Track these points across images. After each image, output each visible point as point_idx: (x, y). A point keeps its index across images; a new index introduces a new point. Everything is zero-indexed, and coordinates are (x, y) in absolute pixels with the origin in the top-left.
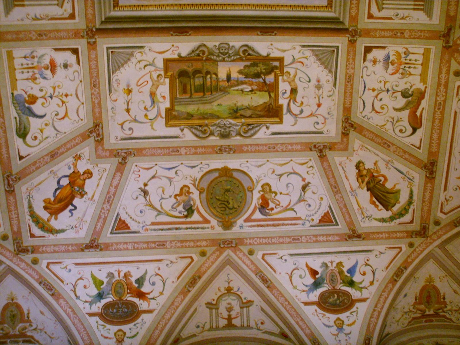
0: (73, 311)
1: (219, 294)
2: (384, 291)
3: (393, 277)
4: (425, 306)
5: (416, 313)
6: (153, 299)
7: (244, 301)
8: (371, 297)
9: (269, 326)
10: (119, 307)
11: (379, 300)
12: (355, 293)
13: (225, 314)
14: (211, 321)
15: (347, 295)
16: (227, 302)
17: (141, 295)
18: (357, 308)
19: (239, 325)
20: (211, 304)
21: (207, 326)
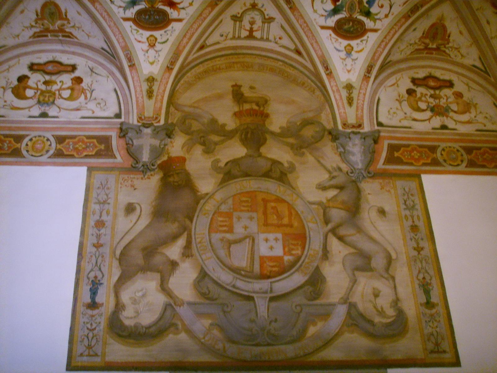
0: (108, 14)
1: (244, 8)
2: (395, 24)
3: (407, 13)
4: (430, 40)
5: (420, 45)
6: (183, 8)
7: (267, 17)
8: (383, 29)
10: (151, 14)
11: (389, 32)
12: (368, 23)
13: (248, 27)
15: (362, 23)
16: (251, 16)
18: (368, 37)
20: (236, 16)
21: (230, 36)
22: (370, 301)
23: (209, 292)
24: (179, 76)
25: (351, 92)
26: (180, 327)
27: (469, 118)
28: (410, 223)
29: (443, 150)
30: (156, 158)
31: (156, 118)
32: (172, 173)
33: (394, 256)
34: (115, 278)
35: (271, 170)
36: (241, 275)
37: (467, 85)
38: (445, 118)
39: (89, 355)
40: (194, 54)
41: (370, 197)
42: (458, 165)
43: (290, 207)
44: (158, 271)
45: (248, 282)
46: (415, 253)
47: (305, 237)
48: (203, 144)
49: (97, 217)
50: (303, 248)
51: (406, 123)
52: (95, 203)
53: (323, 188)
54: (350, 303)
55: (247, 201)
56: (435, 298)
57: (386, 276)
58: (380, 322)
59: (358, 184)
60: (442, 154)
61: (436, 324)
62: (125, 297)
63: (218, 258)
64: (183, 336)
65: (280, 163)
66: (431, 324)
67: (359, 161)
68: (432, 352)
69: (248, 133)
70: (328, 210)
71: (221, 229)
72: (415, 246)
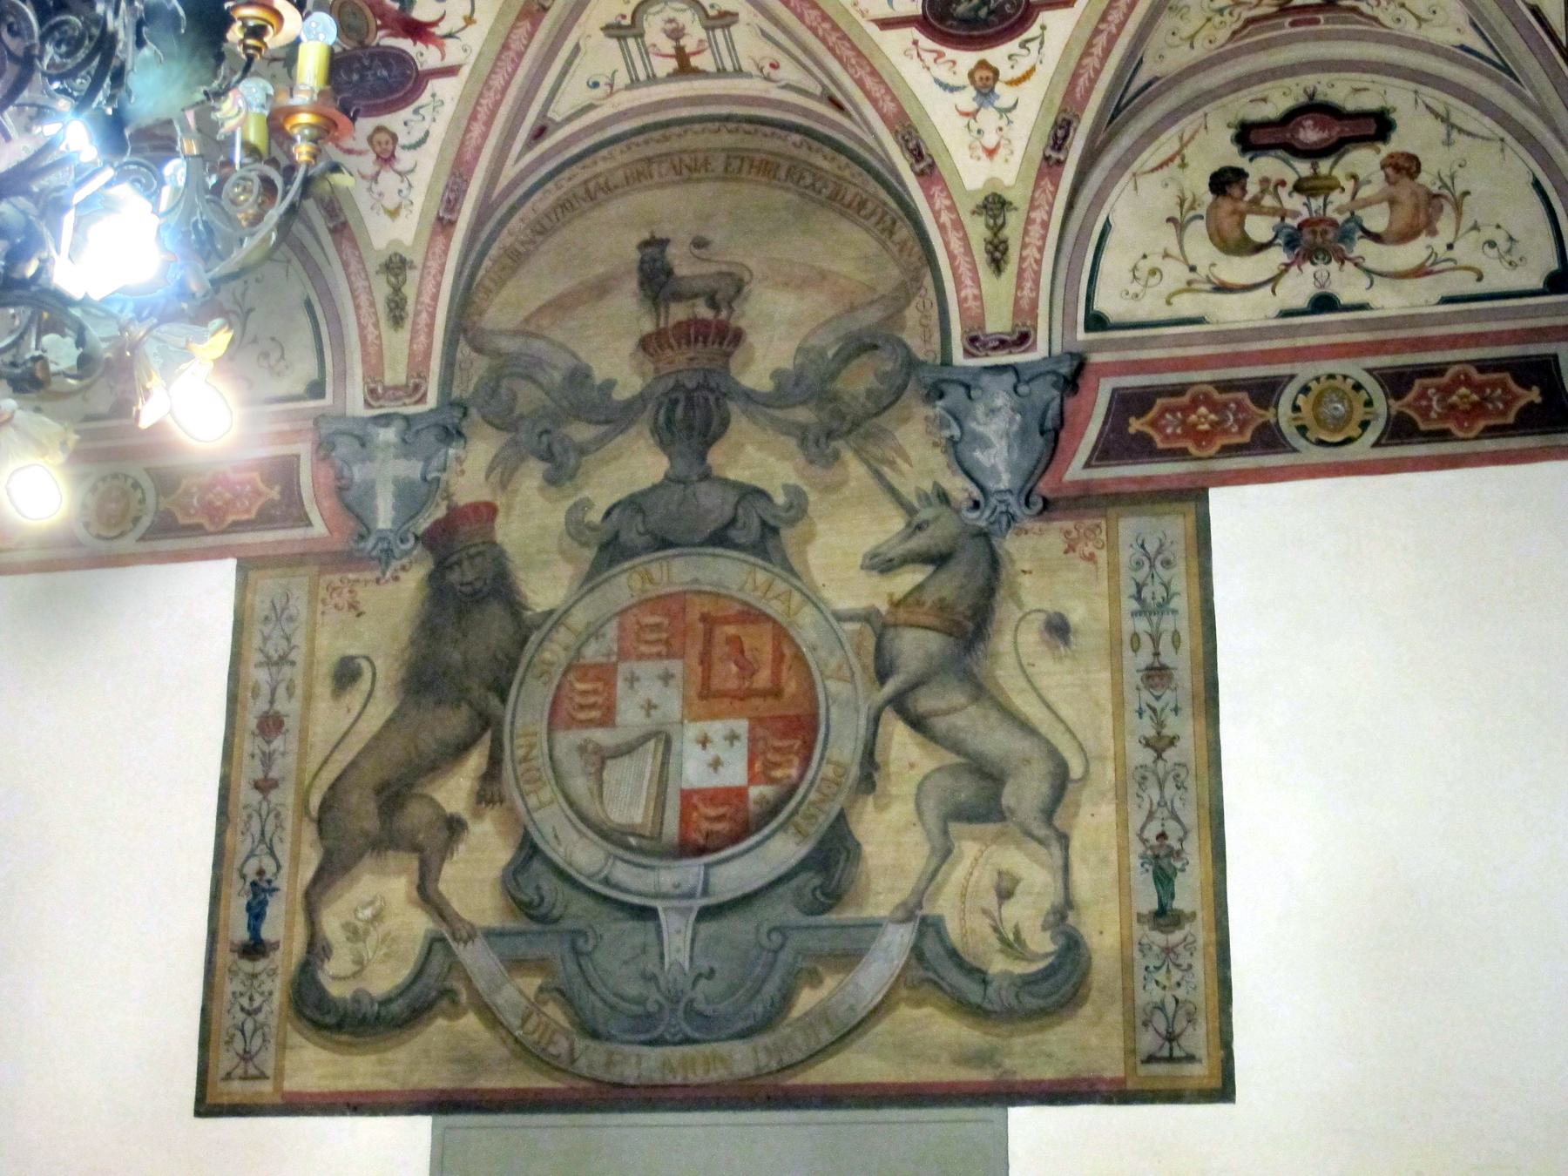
6: (450, 36)
7: (712, 13)
9: (789, 72)
10: (363, 66)
14: (630, 66)
17: (418, 31)
19: (712, 68)
21: (623, 78)
22: (985, 912)
23: (542, 899)
24: (484, 236)
25: (1000, 221)
26: (464, 997)
27: (1425, 254)
28: (1145, 658)
29: (1305, 390)
30: (412, 517)
31: (417, 387)
32: (454, 558)
33: (1076, 769)
34: (308, 873)
35: (733, 522)
36: (629, 848)
37: (1445, 120)
38: (1334, 265)
39: (245, 1077)
40: (517, 160)
41: (1026, 581)
42: (1348, 441)
43: (781, 634)
44: (416, 848)
45: (645, 867)
46: (1149, 755)
47: (815, 730)
48: (548, 456)
49: (262, 705)
50: (806, 761)
51: (1186, 306)
52: (259, 665)
53: (882, 564)
54: (924, 920)
55: (657, 627)
56: (1188, 894)
57: (1042, 832)
58: (1007, 974)
59: (995, 541)
60: (1296, 408)
61: (1176, 975)
62: (332, 924)
63: (571, 804)
64: (470, 1022)
65: (761, 494)
66: (1161, 976)
67: (1001, 468)
68: (1151, 1059)
69: (675, 402)
70: (890, 633)
71: (582, 716)
72: (1150, 732)
